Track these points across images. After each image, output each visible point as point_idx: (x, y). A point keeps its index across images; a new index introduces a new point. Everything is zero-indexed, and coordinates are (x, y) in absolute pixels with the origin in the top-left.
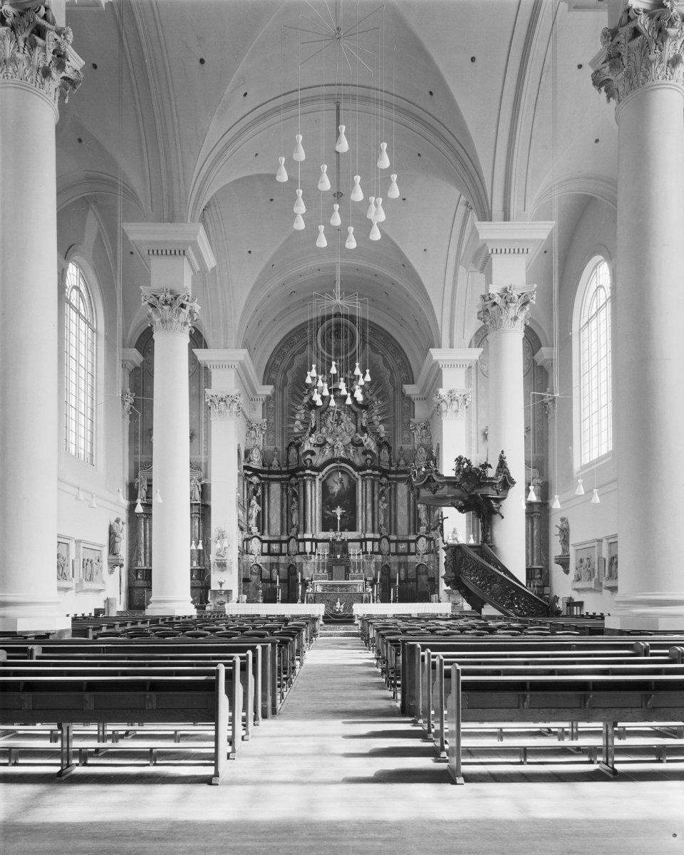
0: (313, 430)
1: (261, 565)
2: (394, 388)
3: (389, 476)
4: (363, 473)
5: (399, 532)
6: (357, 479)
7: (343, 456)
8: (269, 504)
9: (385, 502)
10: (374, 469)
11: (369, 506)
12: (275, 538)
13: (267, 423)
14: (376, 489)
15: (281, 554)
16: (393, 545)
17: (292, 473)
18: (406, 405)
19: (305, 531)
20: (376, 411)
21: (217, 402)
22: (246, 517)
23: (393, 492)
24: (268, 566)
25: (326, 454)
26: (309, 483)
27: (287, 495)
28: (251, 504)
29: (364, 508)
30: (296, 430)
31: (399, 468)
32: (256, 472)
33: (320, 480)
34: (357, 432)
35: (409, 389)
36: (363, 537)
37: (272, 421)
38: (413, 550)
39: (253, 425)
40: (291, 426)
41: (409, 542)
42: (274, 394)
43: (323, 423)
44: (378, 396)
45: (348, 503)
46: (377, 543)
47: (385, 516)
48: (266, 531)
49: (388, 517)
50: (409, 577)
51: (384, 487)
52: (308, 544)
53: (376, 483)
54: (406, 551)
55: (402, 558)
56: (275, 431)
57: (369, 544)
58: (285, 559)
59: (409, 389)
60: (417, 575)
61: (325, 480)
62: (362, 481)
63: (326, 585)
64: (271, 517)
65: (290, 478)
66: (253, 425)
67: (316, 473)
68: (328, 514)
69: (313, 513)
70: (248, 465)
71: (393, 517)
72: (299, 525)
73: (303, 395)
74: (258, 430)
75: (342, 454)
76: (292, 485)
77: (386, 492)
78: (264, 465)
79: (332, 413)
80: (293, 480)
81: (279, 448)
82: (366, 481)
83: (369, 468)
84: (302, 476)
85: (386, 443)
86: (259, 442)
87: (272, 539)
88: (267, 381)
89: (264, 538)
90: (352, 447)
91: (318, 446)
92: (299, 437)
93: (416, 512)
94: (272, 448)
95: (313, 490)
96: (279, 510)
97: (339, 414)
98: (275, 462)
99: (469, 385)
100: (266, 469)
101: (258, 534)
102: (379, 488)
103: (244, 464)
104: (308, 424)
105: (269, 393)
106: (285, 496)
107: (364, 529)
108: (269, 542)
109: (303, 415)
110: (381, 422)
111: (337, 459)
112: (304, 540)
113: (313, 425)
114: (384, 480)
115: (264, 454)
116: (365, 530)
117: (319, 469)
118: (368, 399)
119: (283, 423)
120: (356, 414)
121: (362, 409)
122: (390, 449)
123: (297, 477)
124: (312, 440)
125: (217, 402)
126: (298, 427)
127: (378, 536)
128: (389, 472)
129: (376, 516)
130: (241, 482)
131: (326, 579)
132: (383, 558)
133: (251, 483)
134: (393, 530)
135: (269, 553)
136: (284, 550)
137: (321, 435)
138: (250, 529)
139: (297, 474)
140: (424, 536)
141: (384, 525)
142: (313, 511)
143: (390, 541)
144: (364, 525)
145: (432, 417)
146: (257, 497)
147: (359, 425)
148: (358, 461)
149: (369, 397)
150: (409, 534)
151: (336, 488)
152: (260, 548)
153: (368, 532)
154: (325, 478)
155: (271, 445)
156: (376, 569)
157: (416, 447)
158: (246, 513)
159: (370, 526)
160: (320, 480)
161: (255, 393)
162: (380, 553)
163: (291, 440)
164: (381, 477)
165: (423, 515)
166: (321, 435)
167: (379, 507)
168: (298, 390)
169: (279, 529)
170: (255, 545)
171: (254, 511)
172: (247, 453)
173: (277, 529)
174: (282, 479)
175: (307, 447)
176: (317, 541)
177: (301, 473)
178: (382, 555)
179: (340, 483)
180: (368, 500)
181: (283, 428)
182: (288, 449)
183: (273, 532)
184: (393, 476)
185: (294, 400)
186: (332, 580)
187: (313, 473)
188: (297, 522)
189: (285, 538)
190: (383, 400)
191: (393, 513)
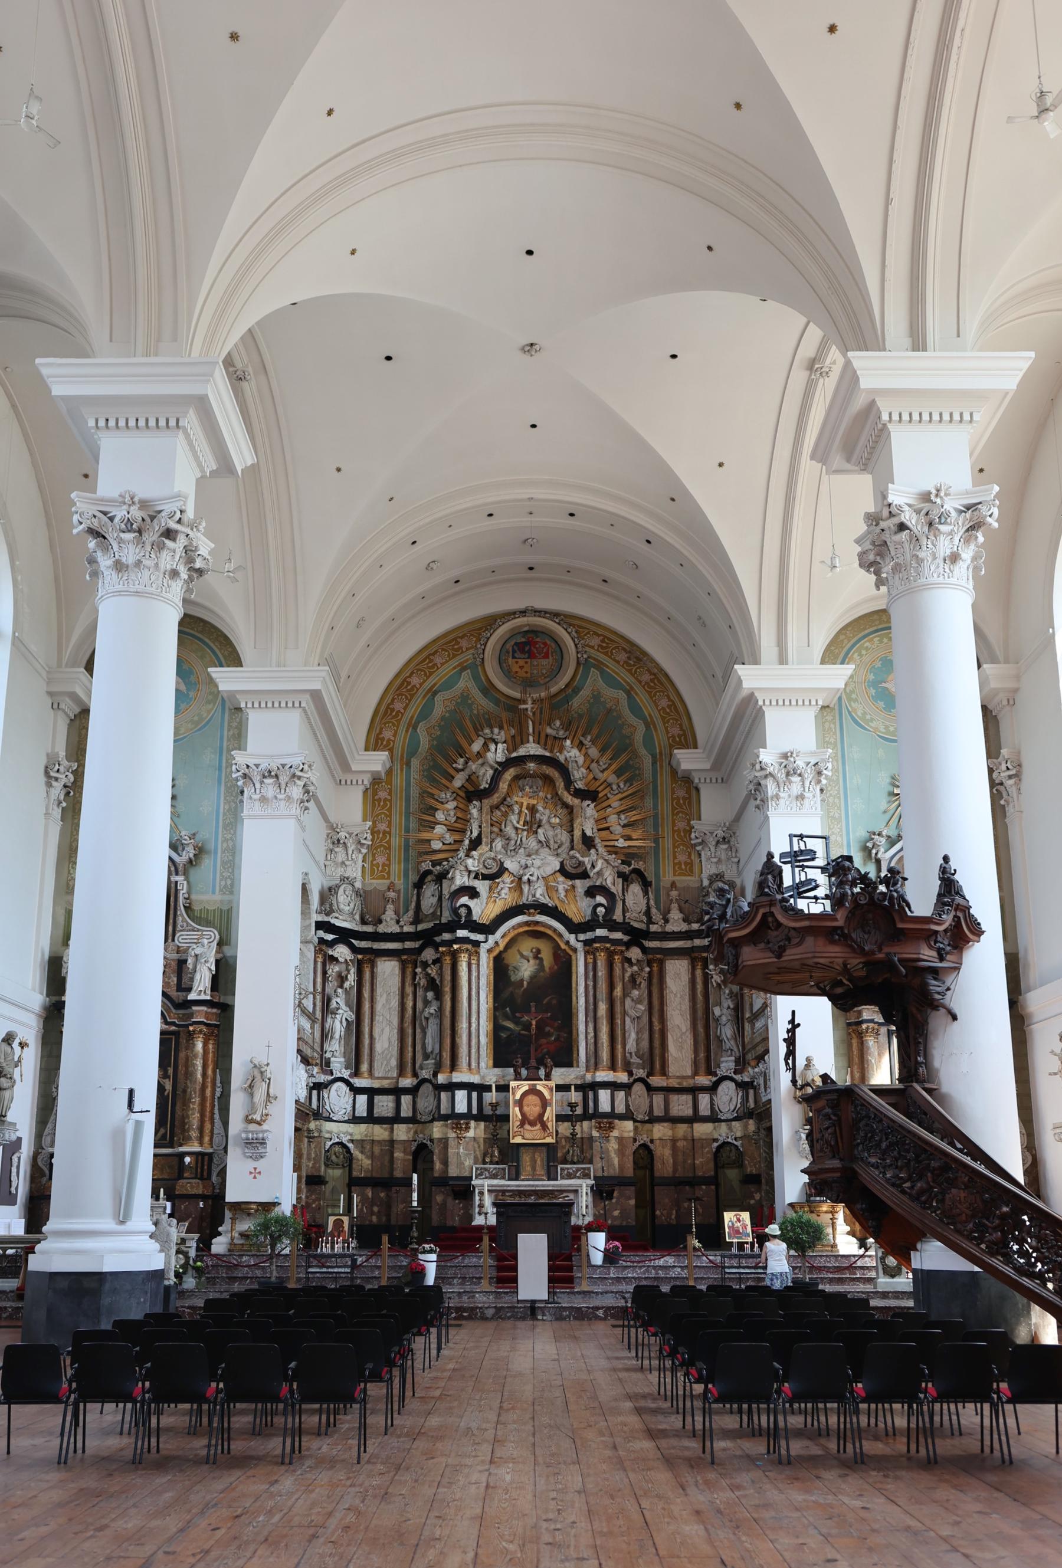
0: (475, 843)
1: (350, 1145)
2: (654, 756)
4: (589, 935)
5: (673, 1069)
6: (575, 950)
7: (543, 900)
8: (372, 1008)
9: (639, 1001)
10: (613, 926)
11: (603, 1008)
12: (386, 1084)
13: (373, 831)
14: (617, 971)
15: (396, 1119)
16: (658, 1099)
17: (427, 938)
18: (681, 793)
19: (454, 1067)
20: (615, 804)
21: (257, 778)
22: (317, 1035)
23: (655, 980)
25: (503, 896)
26: (463, 959)
27: (415, 986)
28: (333, 1005)
29: (591, 1014)
30: (437, 845)
31: (669, 928)
32: (344, 936)
34: (572, 848)
35: (687, 760)
36: (589, 1077)
37: (382, 827)
38: (704, 1109)
39: (342, 834)
40: (425, 835)
41: (694, 1091)
42: (389, 772)
43: (496, 829)
44: (619, 773)
46: (621, 1095)
48: (364, 1067)
51: (635, 968)
52: (461, 1095)
54: (690, 1112)
55: (682, 1129)
56: (389, 848)
57: (604, 1095)
58: (408, 1132)
59: (687, 760)
60: (717, 1167)
61: (501, 952)
62: (587, 953)
63: (504, 1192)
64: (376, 1035)
65: (419, 951)
66: (342, 834)
69: (474, 1026)
70: (326, 919)
72: (441, 1056)
73: (453, 772)
75: (540, 893)
76: (425, 965)
78: (363, 922)
79: (516, 808)
80: (429, 954)
81: (400, 883)
83: (601, 927)
84: (449, 943)
86: (354, 871)
87: (376, 1084)
88: (375, 742)
89: (358, 1082)
90: (561, 879)
91: (485, 877)
92: (446, 859)
94: (381, 884)
95: (474, 974)
96: (395, 1021)
97: (533, 809)
98: (389, 915)
99: (823, 742)
100: (369, 929)
101: (346, 1074)
102: (624, 970)
103: (316, 917)
104: (463, 831)
105: (378, 767)
106: (409, 990)
107: (592, 1061)
108: (371, 1093)
109: (452, 813)
112: (451, 1087)
113: (475, 834)
114: (635, 953)
115: (363, 895)
116: (594, 1064)
117: (488, 929)
118: (595, 779)
119: (407, 830)
120: (570, 809)
122: (646, 884)
123: (436, 946)
124: (472, 864)
125: (257, 778)
126: (439, 836)
127: (623, 1077)
128: (647, 935)
129: (619, 1032)
130: (311, 955)
131: (503, 1178)
132: (636, 1129)
133: (334, 959)
134: (658, 1066)
135: (371, 1118)
136: (406, 1111)
138: (328, 1063)
139: (438, 939)
142: (474, 1020)
144: (592, 1048)
145: (738, 818)
146: (347, 992)
147: (577, 833)
149: (600, 775)
150: (696, 1073)
151: (526, 970)
152: (349, 1109)
153: (600, 1066)
154: (502, 947)
155: (383, 878)
156: (621, 1152)
157: (706, 883)
158: (317, 1027)
159: (605, 1054)
160: (489, 951)
161: (345, 767)
162: (628, 1116)
163: (426, 866)
164: (628, 945)
166: (492, 855)
167: (624, 1013)
168: (441, 760)
170: (338, 1099)
171: (337, 1023)
172: (327, 895)
174: (404, 951)
175: (461, 879)
177: (446, 936)
178: (635, 1121)
179: (536, 957)
180: (599, 996)
181: (407, 841)
182: (419, 885)
185: (433, 781)
186: (517, 1179)
187: (474, 937)
188: (437, 1051)
189: (407, 1082)
190: (629, 781)
191: (657, 1026)
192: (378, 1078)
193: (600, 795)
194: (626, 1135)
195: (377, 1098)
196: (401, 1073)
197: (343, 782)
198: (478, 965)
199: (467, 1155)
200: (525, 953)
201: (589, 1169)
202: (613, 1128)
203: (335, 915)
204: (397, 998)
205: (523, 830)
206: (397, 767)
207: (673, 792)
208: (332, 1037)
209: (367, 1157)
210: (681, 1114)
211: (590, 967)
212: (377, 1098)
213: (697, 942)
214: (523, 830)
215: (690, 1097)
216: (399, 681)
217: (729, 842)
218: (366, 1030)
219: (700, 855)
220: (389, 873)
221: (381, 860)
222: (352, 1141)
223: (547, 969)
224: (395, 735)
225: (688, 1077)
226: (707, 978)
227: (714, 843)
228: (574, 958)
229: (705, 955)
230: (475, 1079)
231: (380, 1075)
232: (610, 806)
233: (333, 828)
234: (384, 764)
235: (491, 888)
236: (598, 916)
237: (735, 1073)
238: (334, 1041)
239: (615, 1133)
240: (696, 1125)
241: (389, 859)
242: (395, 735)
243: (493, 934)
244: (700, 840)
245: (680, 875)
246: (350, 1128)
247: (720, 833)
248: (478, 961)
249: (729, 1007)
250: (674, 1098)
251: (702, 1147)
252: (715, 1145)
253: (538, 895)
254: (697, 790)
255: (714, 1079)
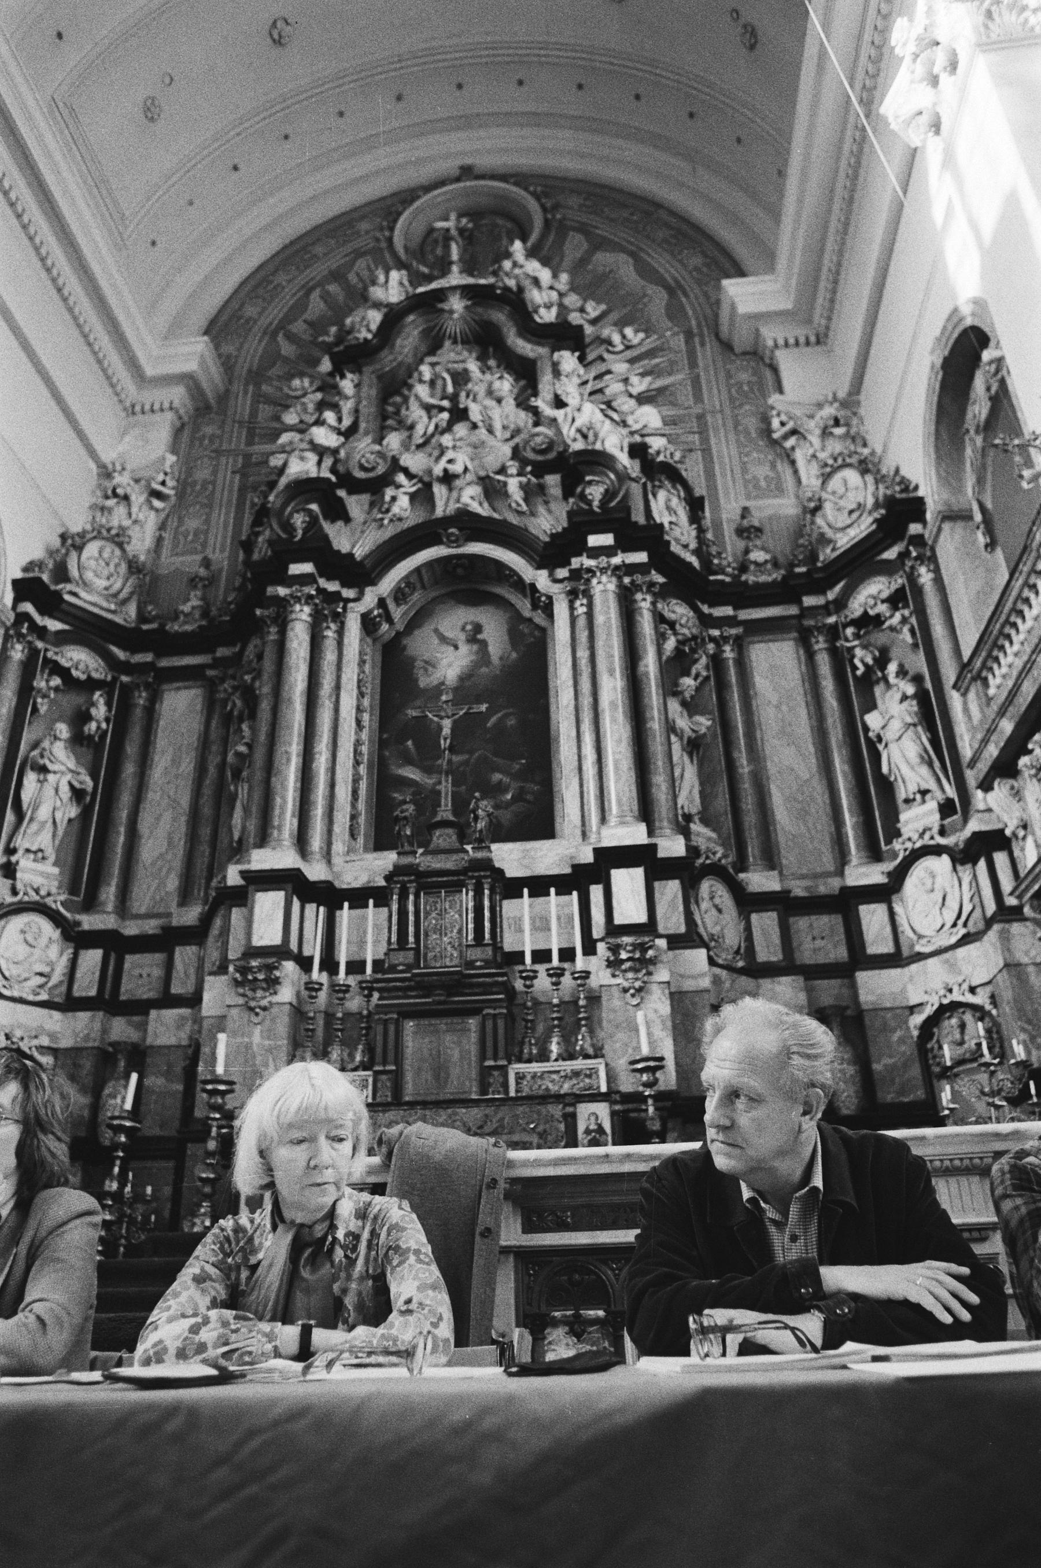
3: (705, 609)
5: (788, 858)
7: (475, 507)
12: (151, 927)
14: (646, 624)
16: (764, 923)
24: (87, 1064)
25: (396, 509)
26: (303, 614)
31: (750, 578)
32: (89, 629)
33: (368, 624)
37: (202, 474)
41: (847, 903)
42: (224, 398)
45: (511, 722)
47: (706, 780)
48: (109, 893)
49: (723, 786)
50: (888, 1096)
52: (269, 905)
53: (644, 603)
54: (840, 953)
61: (399, 634)
62: (573, 595)
64: (144, 826)
67: (348, 593)
68: (404, 783)
71: (746, 786)
74: (138, 498)
77: (701, 666)
82: (588, 594)
85: (672, 474)
86: (141, 543)
87: (131, 929)
89: (89, 922)
93: (864, 752)
95: (330, 656)
96: (185, 801)
97: (461, 378)
108: (114, 945)
110: (642, 399)
111: (447, 521)
117: (359, 574)
121: (555, 349)
127: (672, 846)
132: (716, 981)
135: (108, 1001)
137: (377, 448)
140: (937, 851)
141: (705, 821)
143: (748, 903)
148: (547, 522)
152: (58, 975)
153: (613, 820)
155: (194, 552)
165: (905, 757)
169: (173, 883)
171: (49, 791)
173: (162, 884)
174: (216, 663)
176: (330, 897)
179: (472, 640)
183: (142, 899)
184: (728, 611)
187: (332, 587)
189: (190, 916)
191: (744, 767)
192: (138, 917)
193: (591, 357)
194: (689, 985)
195: (130, 960)
196: (185, 897)
197: (138, 408)
198: (340, 644)
199: (270, 1050)
200: (449, 634)
201: (592, 1073)
202: (653, 961)
203: (69, 587)
204: (193, 754)
205: (442, 409)
206: (237, 387)
207: (729, 376)
208: (31, 819)
209: (83, 1090)
210: (821, 959)
211: (582, 622)
212: (130, 960)
213: (809, 601)
214: (442, 409)
215: (837, 920)
216: (253, 282)
217: (848, 425)
218: (123, 815)
219: (793, 463)
220: (204, 545)
221: (192, 524)
222: (54, 1051)
223: (495, 659)
224: (239, 350)
225: (827, 875)
226: (841, 660)
227: (818, 432)
228: (549, 632)
229: (832, 620)
230: (316, 872)
231: (143, 910)
232: (609, 372)
233: (106, 473)
234: (202, 362)
235: (372, 504)
236: (589, 503)
237: (942, 832)
238: (34, 827)
239: (662, 974)
240: (863, 977)
241: (207, 522)
242: (239, 350)
243: (373, 583)
244: (790, 425)
245: (756, 497)
246: (54, 1021)
247: (829, 411)
248: (341, 633)
249: (904, 698)
250: (801, 924)
251: (886, 1029)
252: (917, 1020)
253: (465, 499)
254: (775, 370)
255: (890, 866)
